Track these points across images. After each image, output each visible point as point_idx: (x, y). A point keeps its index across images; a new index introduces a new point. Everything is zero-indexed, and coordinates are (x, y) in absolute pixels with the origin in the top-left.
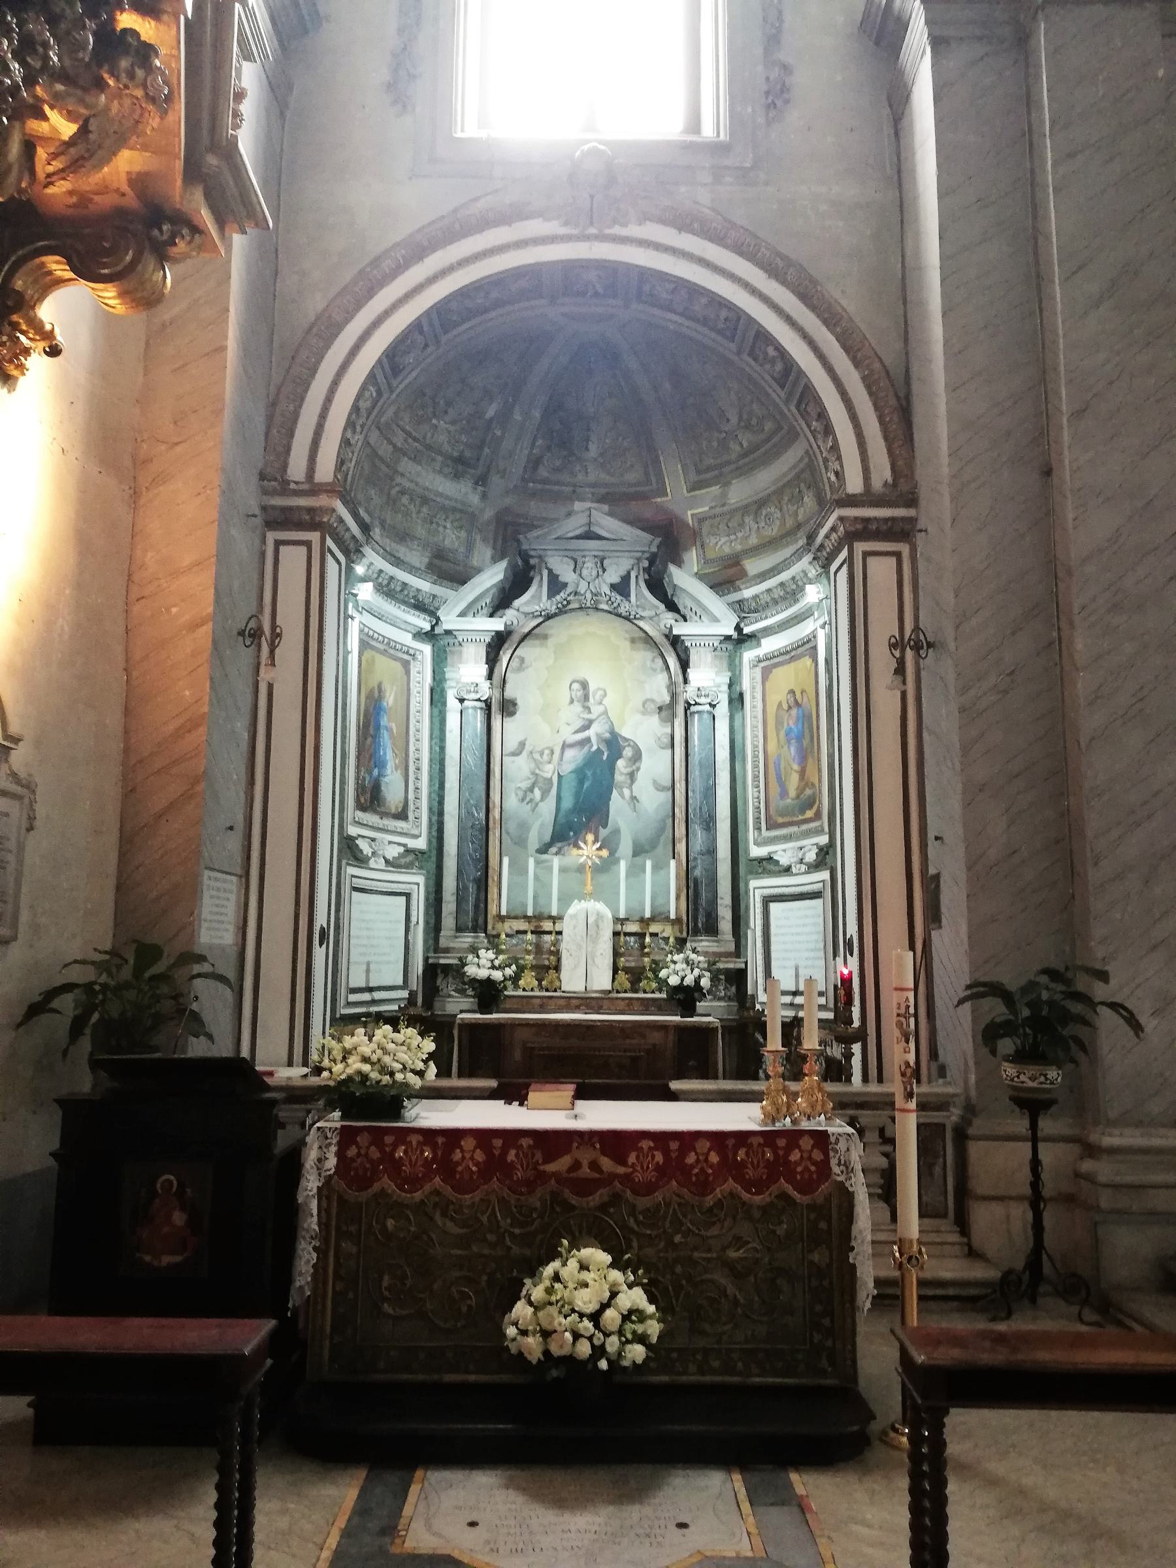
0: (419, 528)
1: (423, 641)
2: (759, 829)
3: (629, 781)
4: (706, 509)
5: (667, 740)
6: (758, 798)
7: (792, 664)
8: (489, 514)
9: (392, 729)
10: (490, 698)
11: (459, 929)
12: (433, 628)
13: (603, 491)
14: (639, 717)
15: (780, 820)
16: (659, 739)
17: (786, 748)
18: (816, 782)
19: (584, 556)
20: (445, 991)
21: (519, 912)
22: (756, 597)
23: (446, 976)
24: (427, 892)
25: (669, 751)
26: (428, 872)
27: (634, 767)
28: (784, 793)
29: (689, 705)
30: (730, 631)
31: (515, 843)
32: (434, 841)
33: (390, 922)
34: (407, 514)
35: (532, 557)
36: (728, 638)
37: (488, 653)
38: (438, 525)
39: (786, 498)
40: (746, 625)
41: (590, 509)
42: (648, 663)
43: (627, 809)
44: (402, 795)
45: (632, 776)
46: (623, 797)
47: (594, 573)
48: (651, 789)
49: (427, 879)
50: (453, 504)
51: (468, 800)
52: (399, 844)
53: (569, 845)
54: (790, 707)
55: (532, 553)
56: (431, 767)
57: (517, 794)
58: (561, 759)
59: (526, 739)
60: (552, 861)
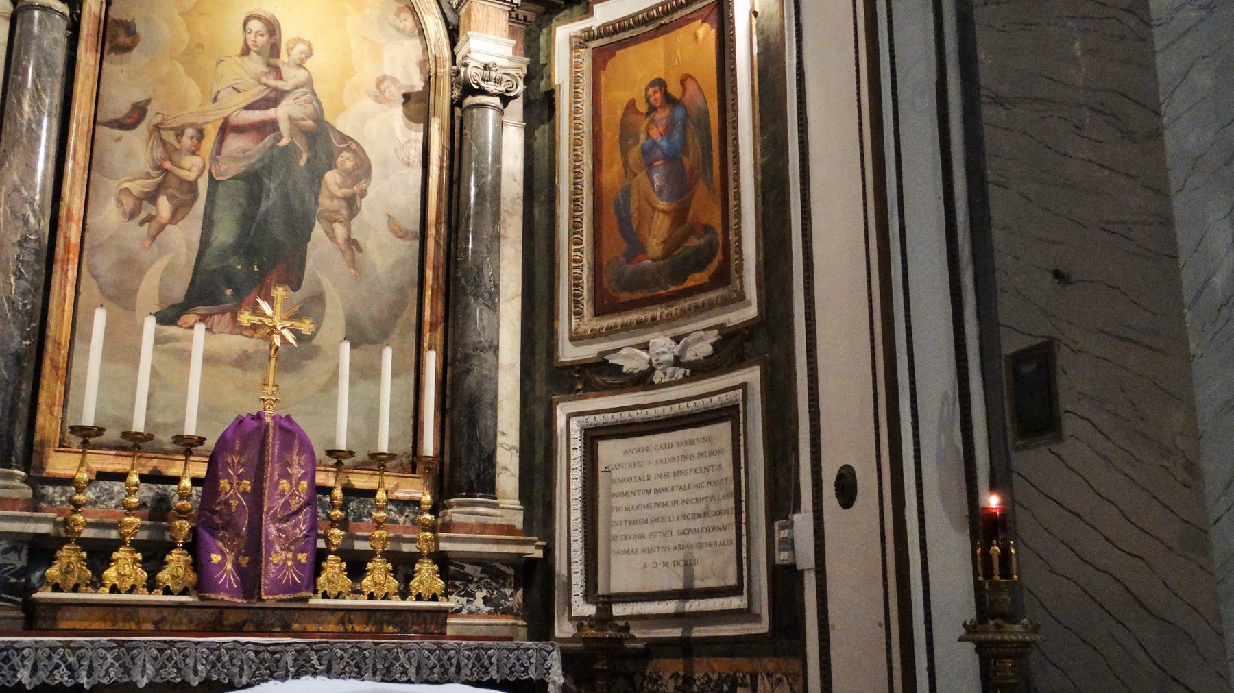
2: (579, 314)
3: (344, 212)
7: (660, 40)
14: (368, 104)
15: (625, 297)
17: (642, 176)
18: (716, 221)
28: (636, 248)
42: (392, 18)
43: (339, 262)
45: (352, 204)
46: (332, 237)
51: (16, 189)
53: (223, 313)
54: (652, 109)
57: (120, 203)
59: (149, 101)
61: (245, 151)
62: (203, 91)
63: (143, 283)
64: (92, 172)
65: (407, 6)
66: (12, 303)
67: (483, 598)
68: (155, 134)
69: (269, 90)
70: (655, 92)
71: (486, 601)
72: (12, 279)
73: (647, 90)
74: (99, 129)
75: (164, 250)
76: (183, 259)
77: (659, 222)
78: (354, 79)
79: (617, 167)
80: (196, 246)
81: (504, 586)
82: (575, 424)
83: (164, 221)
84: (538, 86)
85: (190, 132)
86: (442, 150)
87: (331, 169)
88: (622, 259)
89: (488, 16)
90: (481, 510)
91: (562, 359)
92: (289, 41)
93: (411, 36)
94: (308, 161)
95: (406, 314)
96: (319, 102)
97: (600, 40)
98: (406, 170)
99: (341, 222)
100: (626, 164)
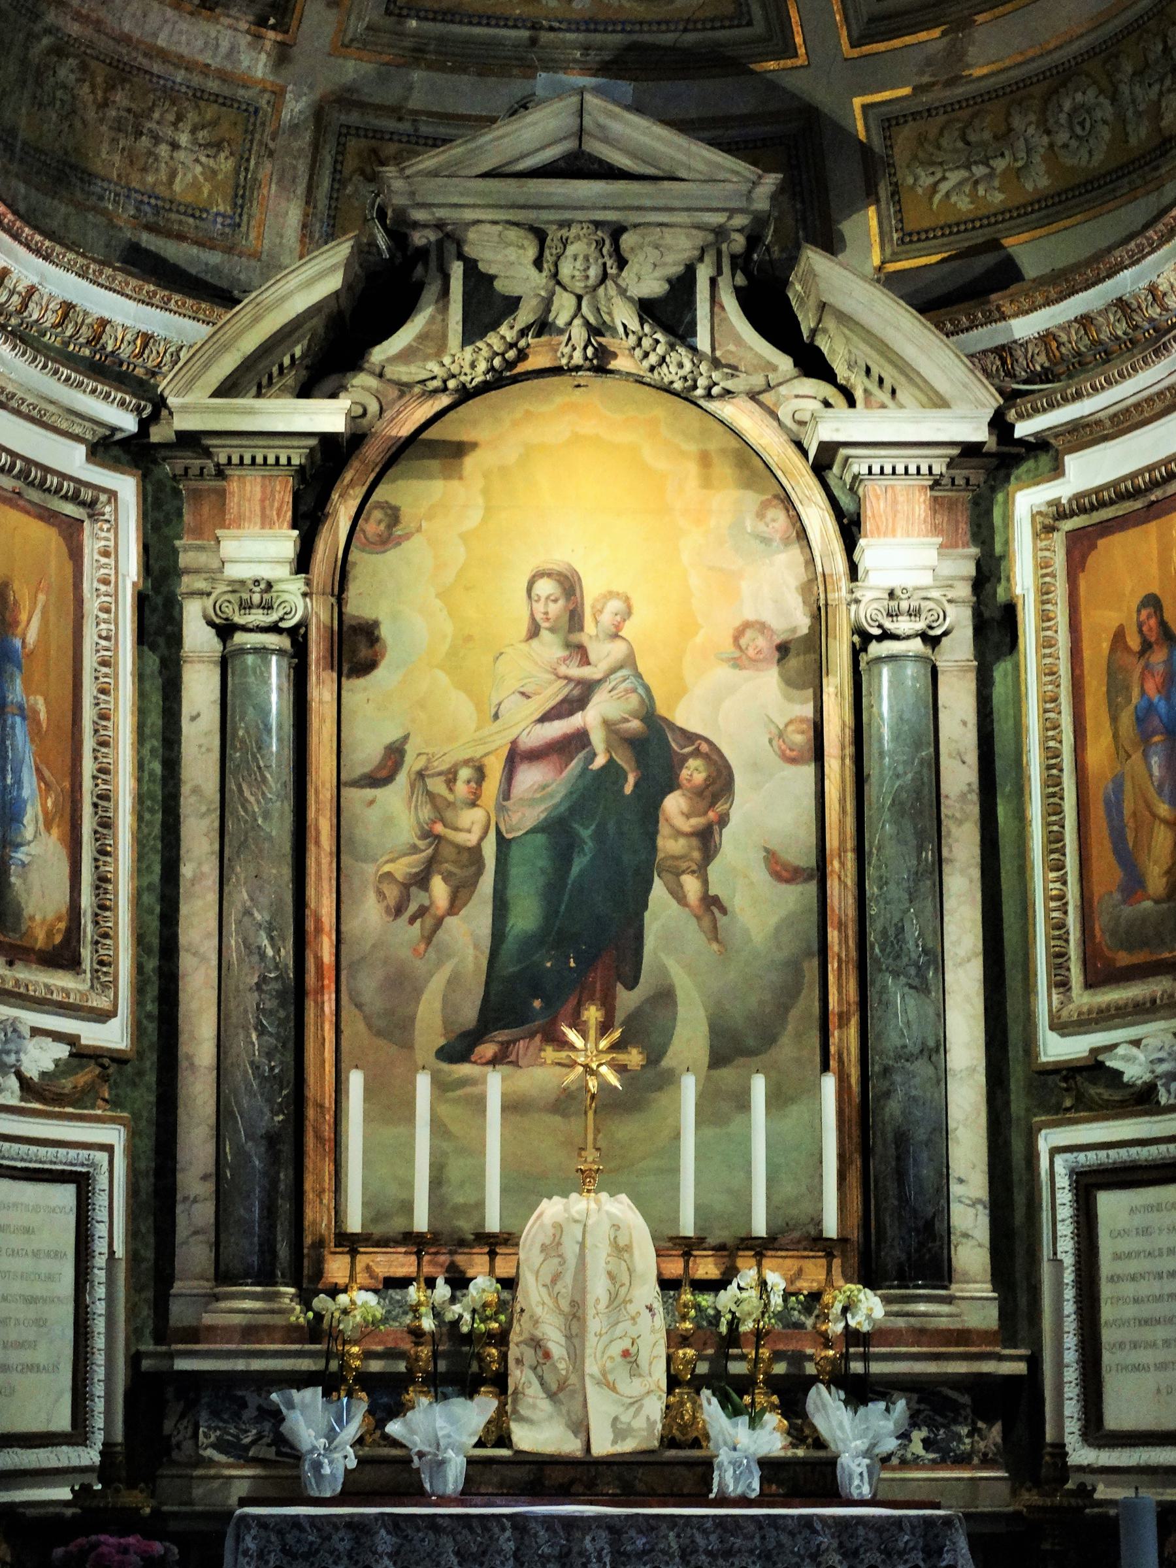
0: (105, 148)
1: (115, 465)
3: (696, 855)
4: (906, 91)
5: (801, 739)
6: (1061, 897)
7: (1153, 526)
8: (295, 107)
9: (36, 712)
10: (303, 624)
11: (224, 1275)
12: (144, 425)
13: (615, 39)
14: (724, 673)
15: (1124, 959)
16: (781, 735)
17: (1137, 756)
19: (566, 224)
20: (188, 1445)
21: (397, 1225)
22: (1046, 338)
23: (191, 1406)
24: (133, 1173)
25: (809, 770)
26: (136, 1117)
27: (711, 815)
28: (1134, 883)
29: (866, 638)
30: (978, 432)
31: (379, 1033)
32: (151, 1027)
33: (36, 1254)
34: (71, 112)
35: (416, 225)
36: (970, 450)
37: (297, 497)
38: (157, 139)
39: (1129, 69)
40: (1021, 416)
41: (581, 92)
42: (749, 525)
43: (693, 935)
44: (59, 899)
46: (680, 898)
47: (594, 272)
48: (760, 875)
49: (133, 1135)
50: (196, 80)
51: (248, 913)
52: (58, 1037)
53: (532, 1036)
54: (1146, 646)
55: (419, 215)
56: (140, 818)
57: (381, 894)
58: (506, 794)
59: (406, 738)
60: (481, 1081)
61: (544, 787)
62: (479, 706)
63: (421, 1008)
64: (343, 857)
65: (776, 497)
66: (256, 1067)
67: (924, 1441)
68: (419, 784)
69: (572, 685)
70: (1148, 617)
71: (927, 1444)
72: (254, 1036)
73: (1139, 611)
74: (346, 792)
75: (444, 955)
76: (470, 966)
77: (1161, 839)
78: (698, 639)
79: (1106, 740)
80: (486, 943)
81: (955, 1421)
82: (1061, 1164)
83: (440, 912)
84: (995, 592)
85: (465, 773)
86: (843, 730)
87: (671, 789)
88: (1117, 896)
89: (895, 502)
90: (922, 1307)
91: (1043, 1059)
92: (596, 600)
93: (786, 542)
94: (636, 785)
95: (801, 1003)
96: (647, 689)
97: (1075, 519)
98: (791, 770)
99: (693, 872)
100: (1116, 736)
